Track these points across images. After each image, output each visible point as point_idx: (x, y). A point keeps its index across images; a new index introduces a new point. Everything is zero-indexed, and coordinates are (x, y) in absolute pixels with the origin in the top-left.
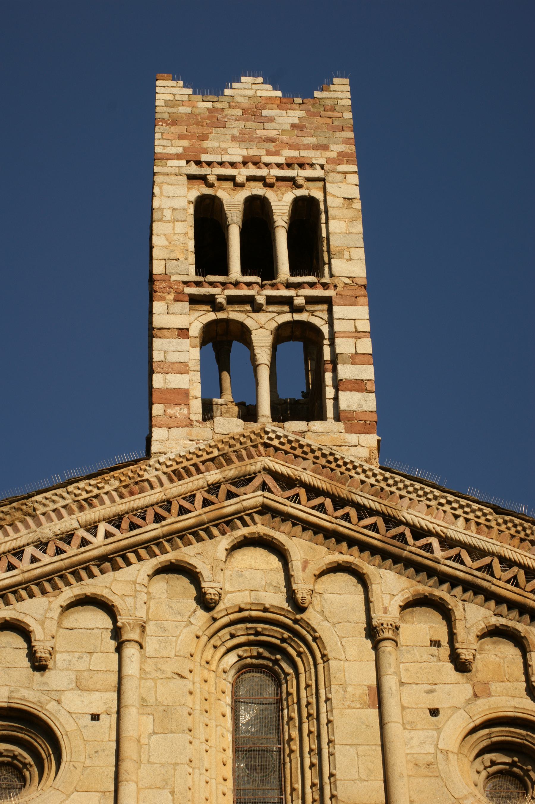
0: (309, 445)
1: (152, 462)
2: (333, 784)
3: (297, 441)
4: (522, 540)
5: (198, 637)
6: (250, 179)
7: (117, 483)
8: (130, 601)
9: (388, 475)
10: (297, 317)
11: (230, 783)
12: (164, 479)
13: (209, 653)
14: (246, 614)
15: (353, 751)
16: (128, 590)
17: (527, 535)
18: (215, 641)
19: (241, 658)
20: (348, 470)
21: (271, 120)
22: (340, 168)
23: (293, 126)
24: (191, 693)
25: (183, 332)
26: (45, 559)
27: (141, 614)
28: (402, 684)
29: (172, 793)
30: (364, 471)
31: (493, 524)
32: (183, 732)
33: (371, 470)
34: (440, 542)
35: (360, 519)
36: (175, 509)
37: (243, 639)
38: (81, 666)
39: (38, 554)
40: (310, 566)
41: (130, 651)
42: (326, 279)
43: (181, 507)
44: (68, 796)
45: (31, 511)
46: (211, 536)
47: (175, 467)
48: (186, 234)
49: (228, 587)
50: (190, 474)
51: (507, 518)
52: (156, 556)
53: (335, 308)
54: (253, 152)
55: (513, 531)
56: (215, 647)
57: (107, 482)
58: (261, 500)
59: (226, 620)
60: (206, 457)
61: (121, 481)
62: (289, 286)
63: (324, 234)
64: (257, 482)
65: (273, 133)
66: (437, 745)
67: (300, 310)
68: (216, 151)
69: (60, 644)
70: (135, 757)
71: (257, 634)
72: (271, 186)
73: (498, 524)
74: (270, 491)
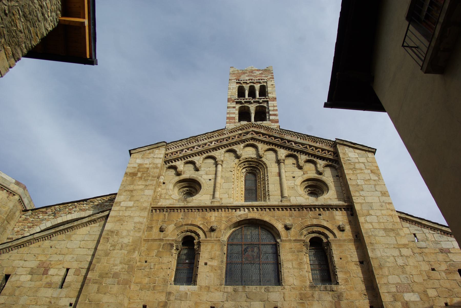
0: (262, 125)
1: (226, 130)
2: (268, 192)
3: (260, 125)
4: (314, 142)
5: (236, 164)
6: (250, 82)
7: (217, 134)
8: (219, 157)
9: (281, 130)
10: (260, 105)
11: (243, 195)
12: (228, 133)
13: (239, 168)
14: (248, 160)
15: (273, 185)
16: (219, 154)
17: (315, 140)
18: (240, 166)
19: (247, 170)
20: (272, 130)
21: (255, 73)
22: (270, 80)
23: (260, 74)
24: (234, 175)
25: (234, 107)
26: (200, 148)
27: (222, 159)
28: (286, 172)
29: (228, 194)
30: (276, 130)
31: (307, 139)
32: (231, 182)
33: (277, 130)
34: (294, 143)
35: (275, 139)
36: (231, 138)
37: (247, 166)
38: (208, 170)
39: (198, 147)
40: (263, 149)
41: (219, 166)
42: (267, 97)
43: (232, 138)
44: (202, 195)
45: (197, 139)
46: (239, 144)
47: (231, 131)
48: (235, 91)
49: (243, 154)
50: (234, 132)
51: (310, 137)
52: (226, 148)
53: (269, 102)
54: (251, 78)
55: (312, 140)
56: (240, 167)
57: (215, 134)
58: (251, 136)
59: (243, 161)
60: (238, 129)
61: (218, 133)
62: (259, 99)
63: (266, 91)
64: (251, 133)
65: (256, 75)
66: (294, 184)
67: (261, 103)
68: (242, 78)
69: (203, 165)
70: (219, 187)
71: (251, 164)
72: (255, 83)
73: (308, 139)
74: (253, 134)
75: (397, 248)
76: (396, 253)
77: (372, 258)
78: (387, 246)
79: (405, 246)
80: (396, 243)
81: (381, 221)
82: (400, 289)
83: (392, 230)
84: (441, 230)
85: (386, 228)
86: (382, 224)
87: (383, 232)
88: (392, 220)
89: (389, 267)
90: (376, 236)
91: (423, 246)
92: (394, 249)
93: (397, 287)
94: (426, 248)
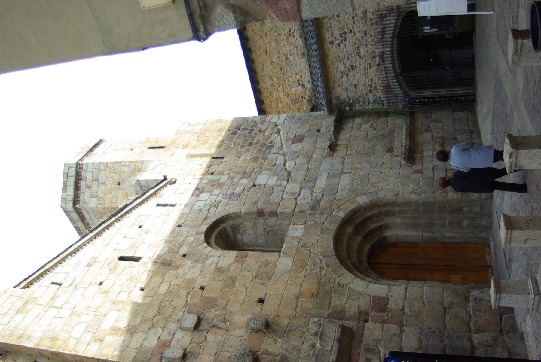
75: (49, 308)
76: (53, 312)
77: (37, 345)
78: (38, 319)
79: (53, 298)
80: (42, 307)
81: (5, 311)
82: (94, 329)
83: (26, 303)
84: (70, 254)
85: (18, 309)
86: (10, 312)
87: (20, 315)
88: (16, 298)
89: (62, 328)
90: (16, 327)
91: (71, 282)
92: (47, 312)
93: (89, 331)
94: (75, 279)
